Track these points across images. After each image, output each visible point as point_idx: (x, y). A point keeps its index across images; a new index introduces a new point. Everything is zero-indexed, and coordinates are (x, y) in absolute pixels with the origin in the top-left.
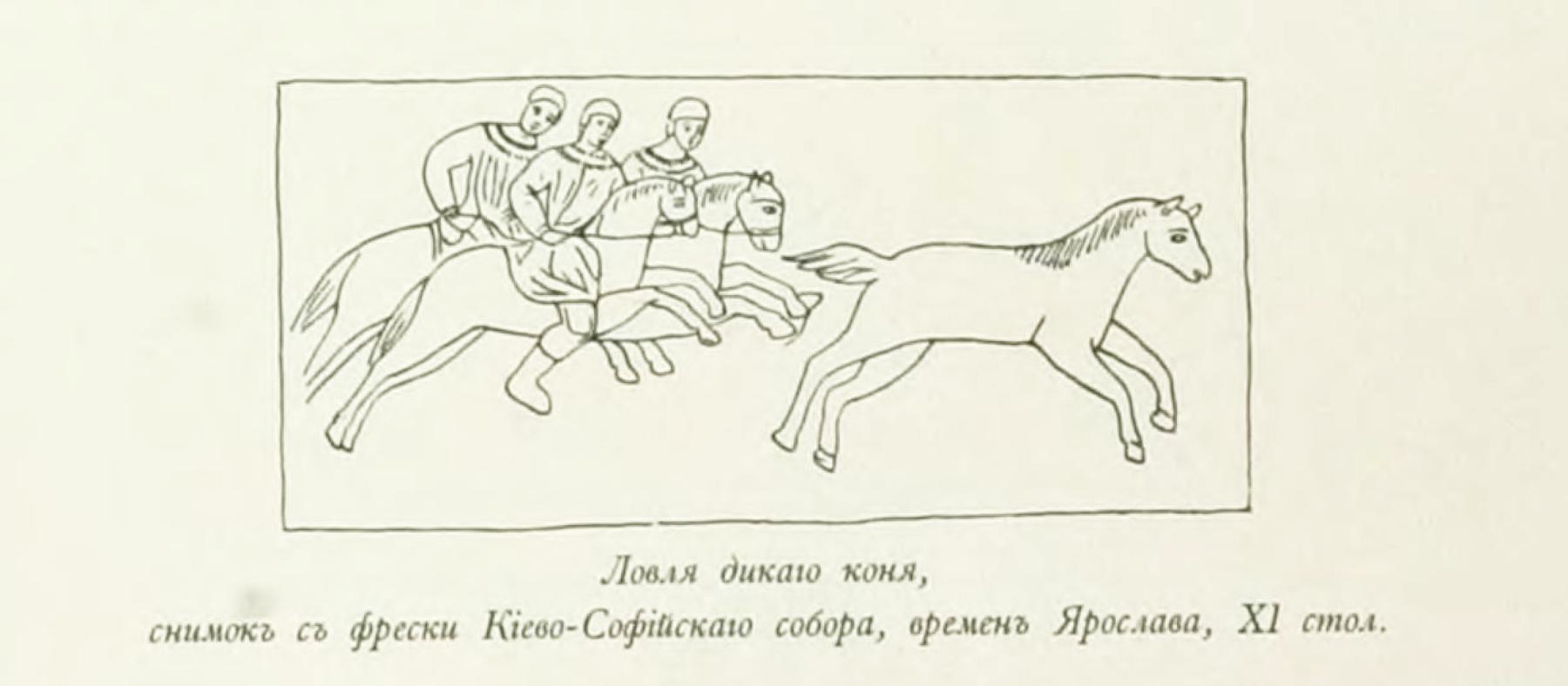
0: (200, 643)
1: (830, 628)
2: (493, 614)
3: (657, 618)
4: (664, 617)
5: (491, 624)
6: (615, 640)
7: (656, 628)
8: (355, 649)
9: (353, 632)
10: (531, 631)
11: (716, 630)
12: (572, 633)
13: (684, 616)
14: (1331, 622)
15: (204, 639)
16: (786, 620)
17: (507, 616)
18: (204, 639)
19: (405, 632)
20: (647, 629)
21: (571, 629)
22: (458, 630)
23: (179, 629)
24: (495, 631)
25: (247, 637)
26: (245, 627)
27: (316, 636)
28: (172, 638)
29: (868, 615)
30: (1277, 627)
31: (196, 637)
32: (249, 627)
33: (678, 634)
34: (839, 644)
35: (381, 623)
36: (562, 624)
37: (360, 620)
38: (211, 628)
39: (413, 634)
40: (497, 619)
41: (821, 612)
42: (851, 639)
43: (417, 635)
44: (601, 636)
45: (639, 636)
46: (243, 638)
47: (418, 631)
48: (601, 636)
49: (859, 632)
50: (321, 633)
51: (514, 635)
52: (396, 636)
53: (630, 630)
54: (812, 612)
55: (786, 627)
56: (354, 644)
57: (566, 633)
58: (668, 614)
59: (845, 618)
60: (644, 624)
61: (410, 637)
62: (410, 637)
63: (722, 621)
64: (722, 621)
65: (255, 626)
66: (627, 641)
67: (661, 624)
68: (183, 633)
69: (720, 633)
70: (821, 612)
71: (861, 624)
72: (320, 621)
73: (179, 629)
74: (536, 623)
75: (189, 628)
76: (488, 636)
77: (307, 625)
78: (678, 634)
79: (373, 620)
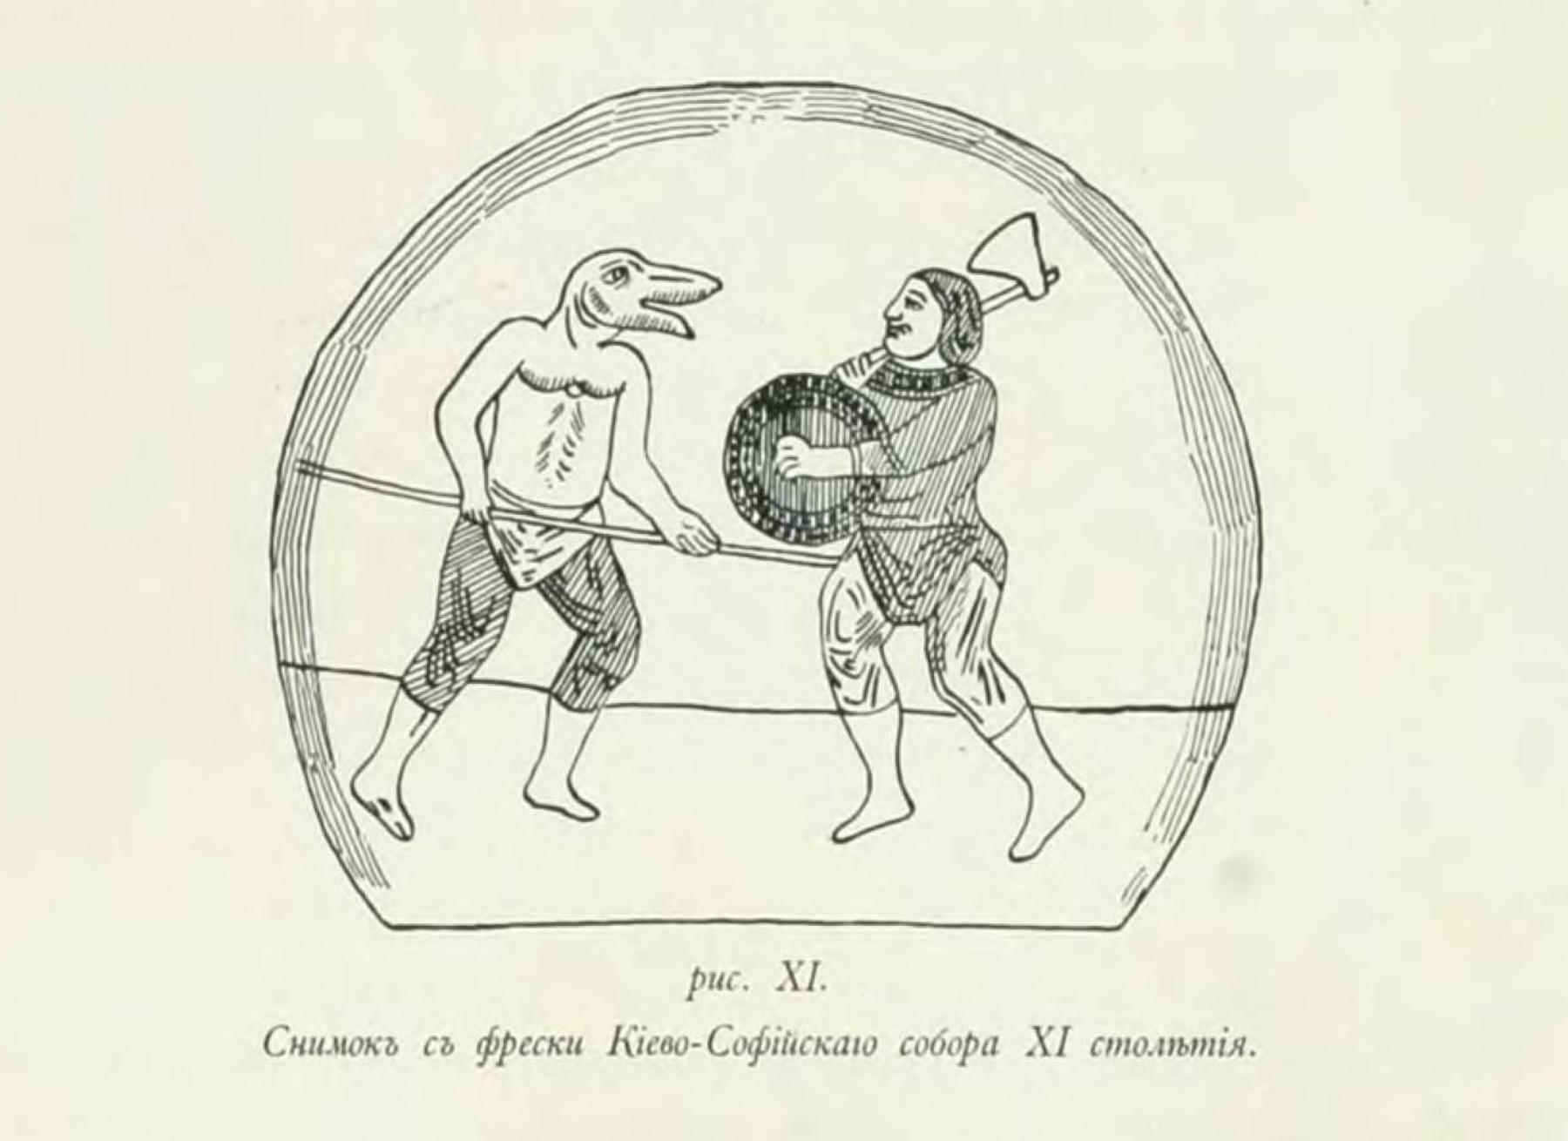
0: (324, 1056)
2: (618, 1029)
3: (782, 1035)
4: (789, 1033)
5: (616, 1040)
6: (740, 1058)
7: (780, 1047)
8: (481, 1065)
9: (479, 1046)
11: (840, 1048)
12: (696, 1049)
15: (329, 1052)
16: (911, 1038)
17: (633, 1033)
18: (329, 1052)
19: (533, 1044)
21: (696, 1045)
22: (583, 1046)
23: (304, 1040)
24: (621, 1046)
25: (371, 1051)
26: (369, 1040)
27: (443, 1050)
28: (297, 1051)
31: (320, 1051)
32: (373, 1040)
33: (802, 1052)
34: (963, 1064)
35: (508, 1037)
36: (687, 1040)
37: (486, 1034)
38: (336, 1040)
39: (539, 1049)
40: (622, 1035)
41: (944, 1031)
42: (975, 1058)
43: (543, 1050)
44: (725, 1053)
46: (366, 1052)
47: (544, 1046)
48: (725, 1053)
49: (984, 1053)
50: (448, 1047)
51: (639, 1051)
52: (522, 1053)
54: (937, 1030)
55: (910, 1045)
56: (480, 1059)
57: (690, 1049)
58: (792, 1032)
59: (970, 1038)
60: (769, 1043)
61: (535, 1052)
62: (535, 1052)
63: (847, 1039)
64: (847, 1039)
65: (379, 1039)
66: (751, 1059)
67: (786, 1041)
68: (307, 1047)
69: (845, 1051)
70: (944, 1031)
71: (986, 1044)
72: (446, 1032)
73: (304, 1040)
75: (314, 1041)
76: (613, 1052)
77: (435, 1038)
78: (802, 1052)
79: (500, 1034)
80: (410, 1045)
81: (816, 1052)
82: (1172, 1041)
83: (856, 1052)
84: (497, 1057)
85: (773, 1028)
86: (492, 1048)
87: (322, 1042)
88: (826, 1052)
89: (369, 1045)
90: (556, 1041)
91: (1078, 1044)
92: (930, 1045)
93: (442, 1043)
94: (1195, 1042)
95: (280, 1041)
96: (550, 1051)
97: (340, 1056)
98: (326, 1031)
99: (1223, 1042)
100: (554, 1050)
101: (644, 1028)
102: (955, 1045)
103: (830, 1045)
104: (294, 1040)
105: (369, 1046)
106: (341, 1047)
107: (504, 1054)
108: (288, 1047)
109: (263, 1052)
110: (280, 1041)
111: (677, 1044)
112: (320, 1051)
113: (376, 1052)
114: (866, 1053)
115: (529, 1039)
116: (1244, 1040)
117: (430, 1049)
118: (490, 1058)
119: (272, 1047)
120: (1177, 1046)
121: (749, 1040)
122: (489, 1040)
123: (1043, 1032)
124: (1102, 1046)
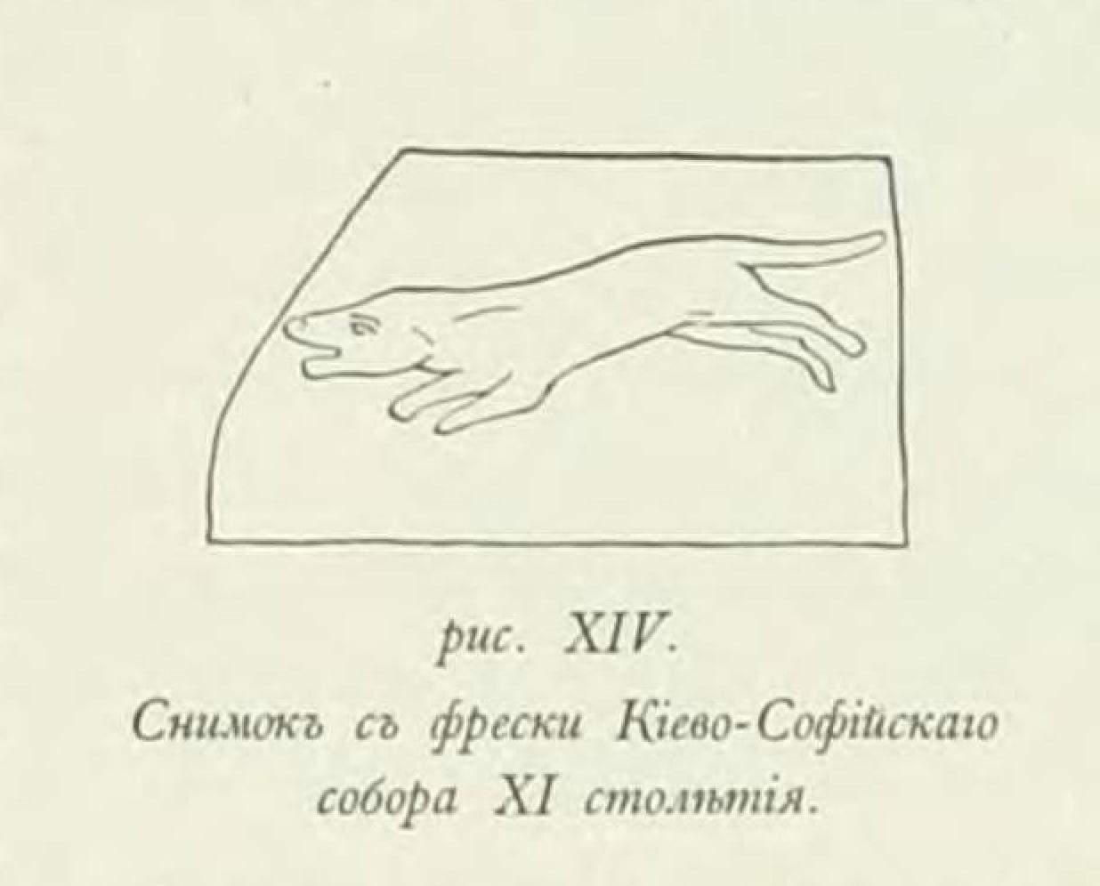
0: (219, 739)
3: (863, 711)
4: (873, 710)
5: (628, 718)
8: (438, 751)
9: (434, 729)
10: (684, 729)
11: (945, 729)
12: (742, 731)
13: (900, 711)
15: (225, 735)
17: (651, 709)
18: (225, 735)
20: (850, 725)
21: (741, 726)
24: (634, 728)
25: (284, 732)
26: (281, 718)
28: (180, 733)
31: (212, 733)
33: (892, 735)
36: (727, 719)
37: (445, 710)
38: (234, 719)
40: (636, 711)
44: (784, 736)
46: (278, 734)
47: (526, 727)
48: (784, 736)
50: (389, 727)
51: (661, 734)
52: (495, 736)
56: (436, 744)
57: (734, 731)
58: (878, 707)
60: (845, 721)
62: (514, 735)
64: (955, 717)
65: (295, 717)
66: (820, 744)
67: (869, 719)
68: (195, 725)
69: (952, 734)
73: (190, 720)
74: (692, 717)
75: (203, 718)
76: (623, 735)
78: (892, 735)
79: (464, 711)
80: (338, 723)
81: (912, 734)
84: (459, 742)
85: (852, 702)
86: (452, 729)
87: (216, 720)
88: (925, 735)
89: (281, 724)
93: (382, 722)
96: (535, 734)
97: (240, 740)
98: (221, 706)
101: (667, 703)
103: (931, 726)
104: (176, 720)
105: (281, 725)
106: (241, 727)
107: (469, 737)
108: (168, 728)
109: (134, 736)
111: (715, 725)
112: (212, 733)
113: (291, 734)
114: (981, 735)
115: (507, 718)
117: (365, 730)
118: (449, 744)
119: (145, 728)
122: (448, 718)
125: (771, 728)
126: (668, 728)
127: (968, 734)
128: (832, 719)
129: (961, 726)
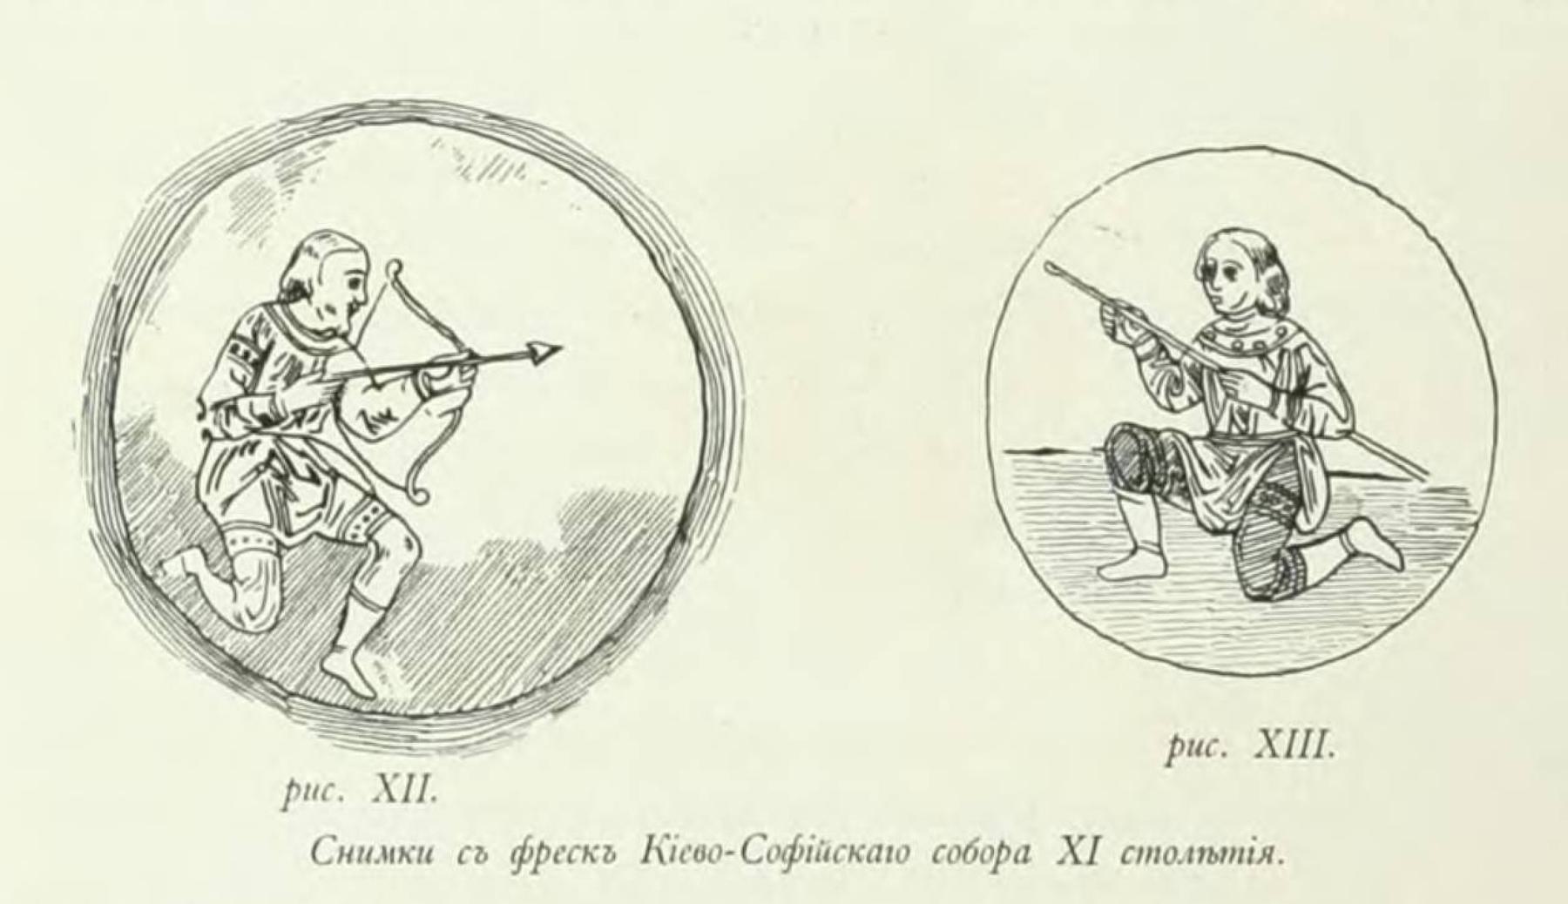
1: (986, 856)
2: (651, 838)
3: (815, 843)
4: (822, 842)
5: (649, 848)
10: (689, 855)
12: (731, 857)
14: (1151, 854)
16: (943, 847)
17: (665, 840)
21: (730, 853)
23: (351, 851)
24: (653, 855)
28: (345, 859)
29: (1025, 842)
30: (1096, 859)
33: (836, 860)
34: (995, 871)
38: (384, 849)
39: (573, 857)
40: (655, 842)
41: (977, 840)
42: (1007, 867)
44: (759, 860)
45: (797, 861)
49: (1016, 861)
51: (672, 859)
53: (787, 857)
55: (943, 853)
57: (724, 857)
58: (826, 839)
59: (1002, 846)
62: (570, 860)
63: (880, 848)
64: (880, 848)
66: (785, 866)
68: (356, 855)
69: (878, 859)
70: (977, 840)
73: (351, 851)
75: (362, 850)
76: (646, 860)
78: (836, 860)
82: (1202, 850)
83: (889, 860)
88: (859, 860)
90: (590, 849)
91: (1108, 854)
92: (963, 854)
94: (1224, 851)
95: (327, 850)
99: (1252, 851)
100: (588, 859)
101: (677, 836)
102: (988, 852)
103: (863, 853)
104: (342, 849)
106: (387, 855)
108: (337, 855)
110: (327, 850)
116: (1272, 849)
119: (321, 856)
120: (1208, 855)
121: (782, 849)
123: (1074, 841)
124: (1132, 855)
125: (752, 853)
126: (678, 854)
127: (889, 860)
128: (794, 848)
129: (884, 854)
